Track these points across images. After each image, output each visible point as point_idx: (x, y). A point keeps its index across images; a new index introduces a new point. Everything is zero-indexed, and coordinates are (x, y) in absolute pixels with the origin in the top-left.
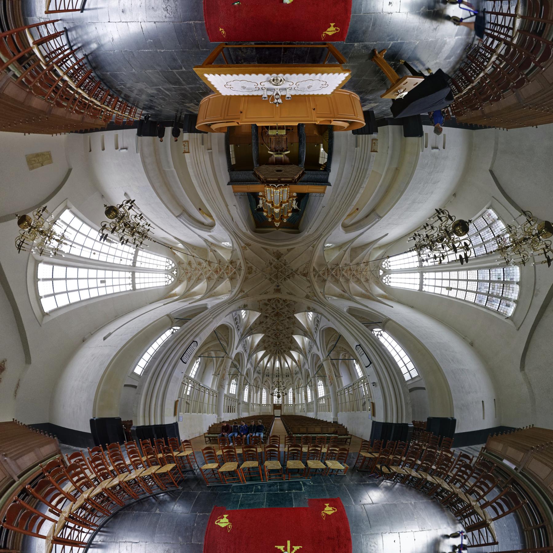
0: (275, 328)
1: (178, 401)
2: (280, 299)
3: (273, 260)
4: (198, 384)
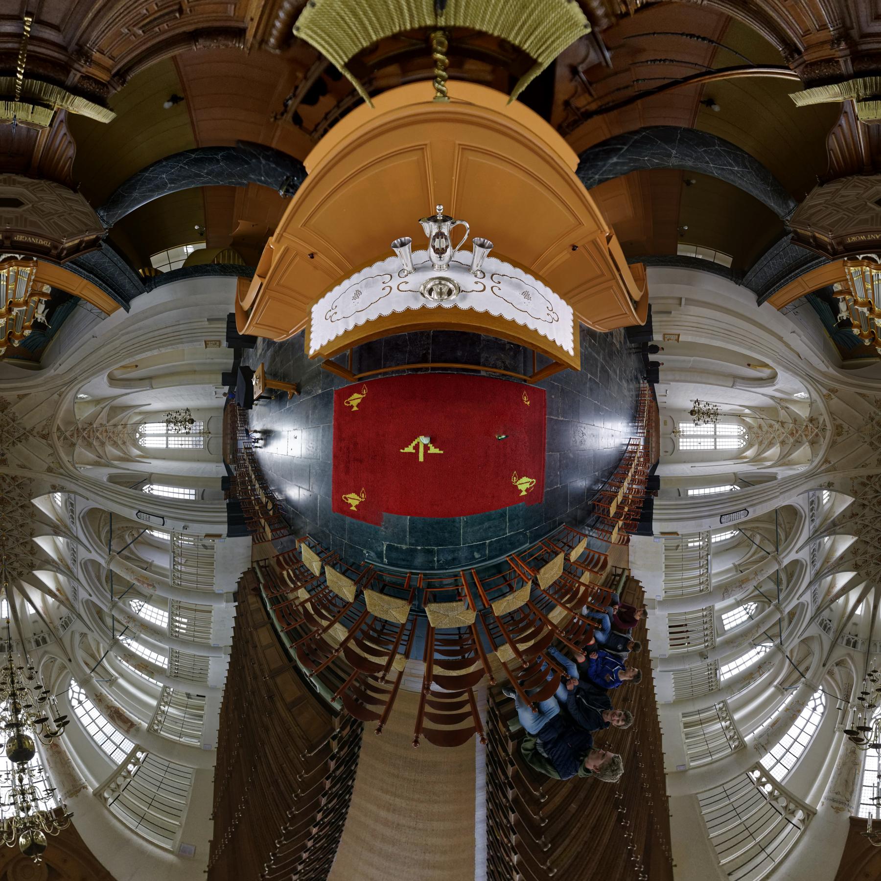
1: (678, 535)
4: (708, 553)
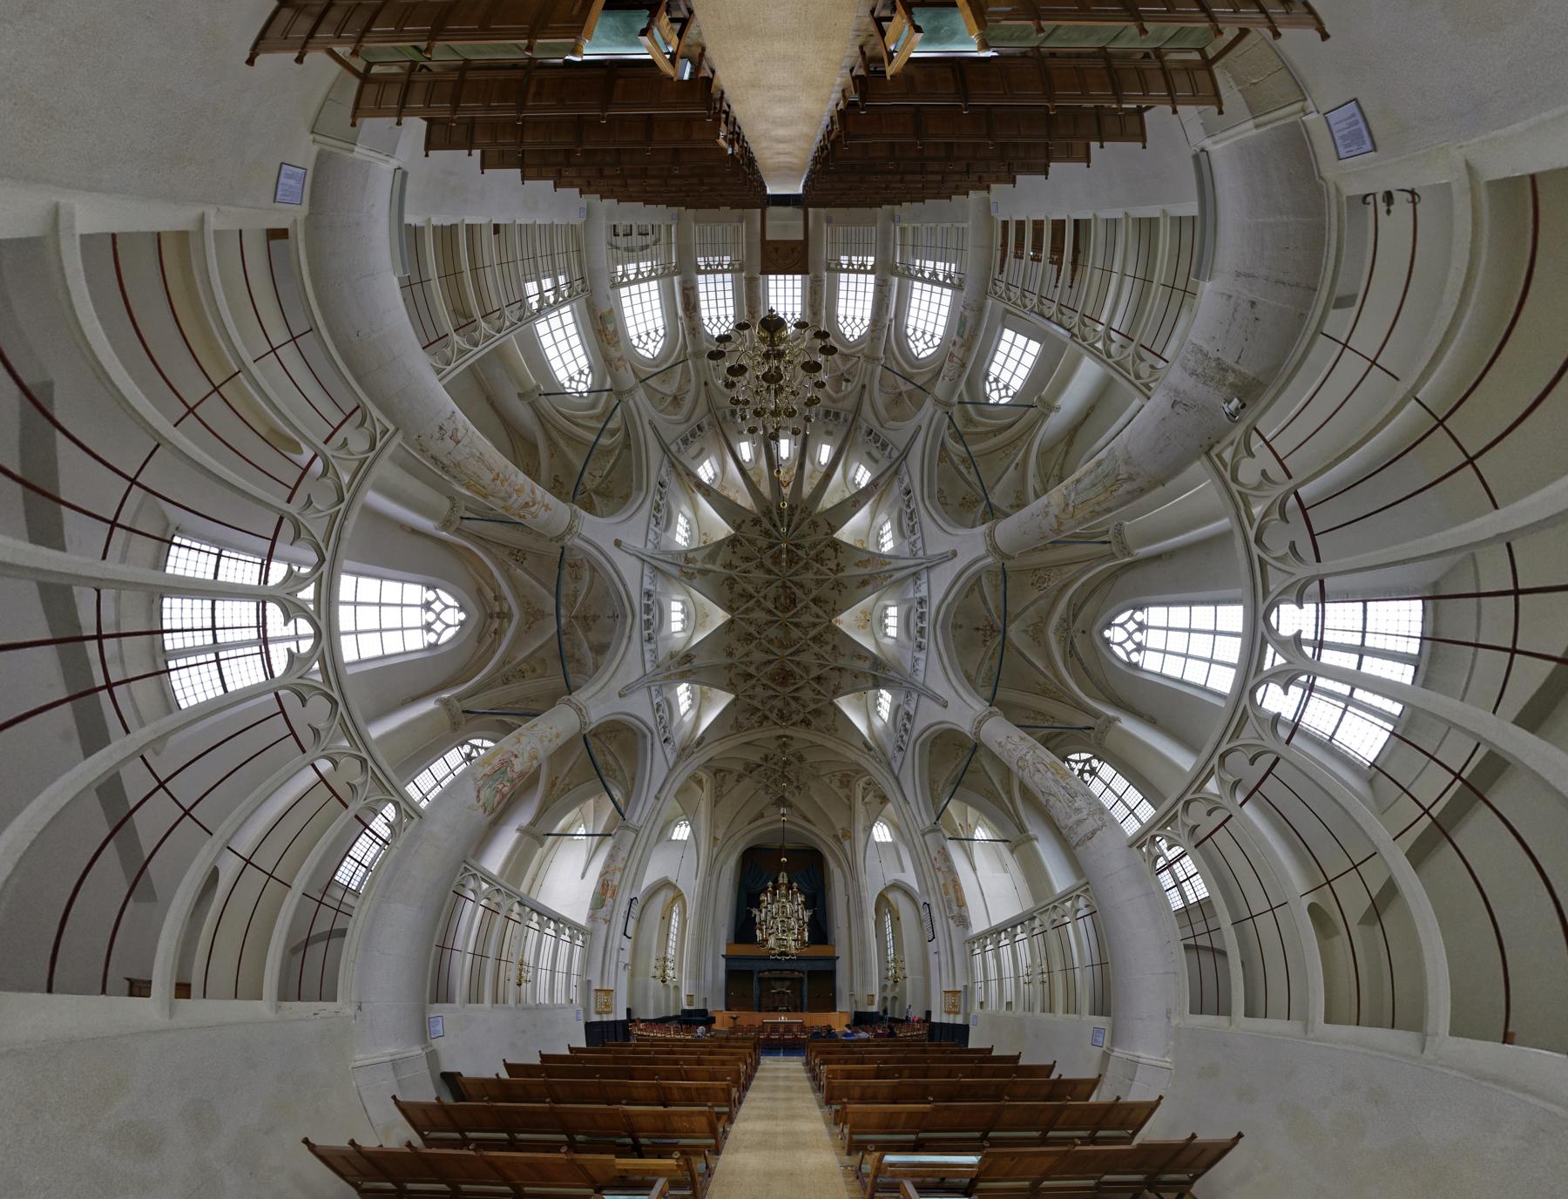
0: (796, 633)
2: (776, 724)
3: (794, 794)
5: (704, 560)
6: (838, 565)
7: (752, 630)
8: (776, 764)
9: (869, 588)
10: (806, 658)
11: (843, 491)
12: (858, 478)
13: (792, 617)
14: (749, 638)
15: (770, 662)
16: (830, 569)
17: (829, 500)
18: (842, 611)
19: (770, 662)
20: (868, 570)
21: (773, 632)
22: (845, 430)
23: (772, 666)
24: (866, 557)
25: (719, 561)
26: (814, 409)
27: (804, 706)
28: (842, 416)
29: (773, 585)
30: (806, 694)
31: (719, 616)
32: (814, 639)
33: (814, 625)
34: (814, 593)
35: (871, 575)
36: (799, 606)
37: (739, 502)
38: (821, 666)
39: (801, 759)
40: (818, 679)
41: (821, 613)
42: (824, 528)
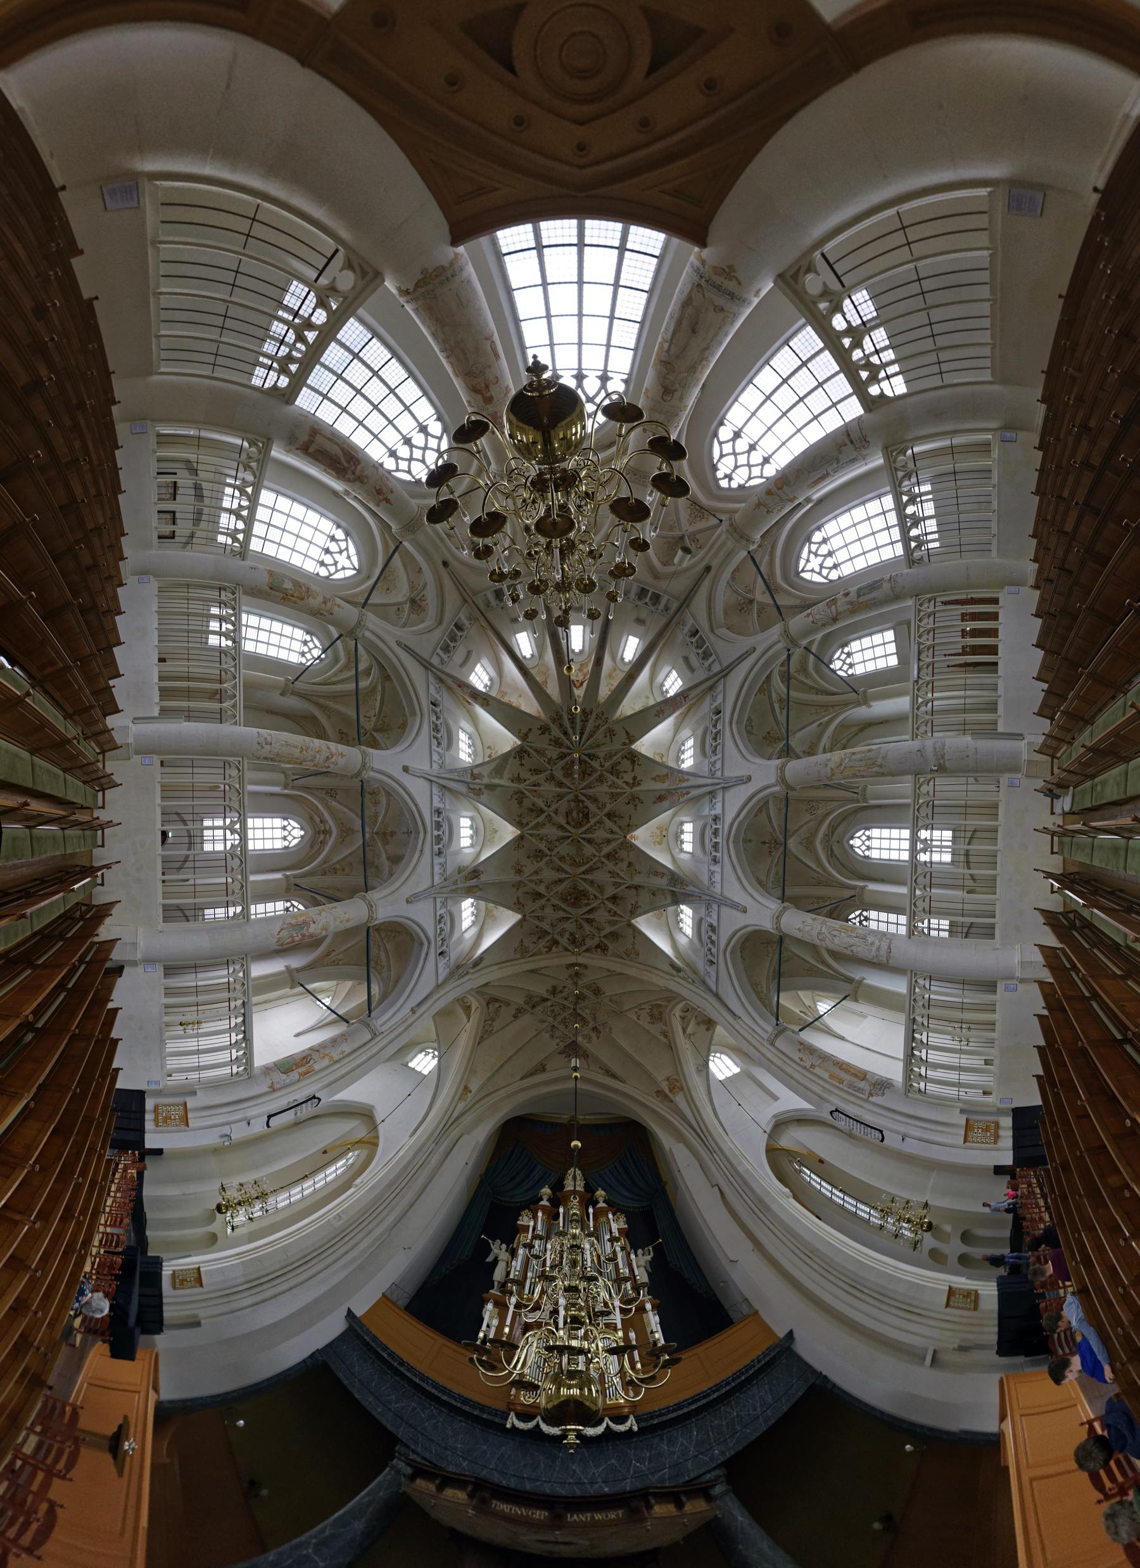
0: (589, 850)
2: (567, 950)
5: (490, 775)
6: (635, 778)
7: (542, 846)
8: (566, 999)
9: (666, 803)
10: (601, 876)
11: (647, 697)
12: (667, 684)
13: (585, 833)
14: (539, 855)
15: (561, 881)
16: (626, 783)
17: (629, 706)
18: (637, 827)
19: (561, 881)
20: (665, 786)
21: (564, 849)
22: (663, 621)
23: (564, 885)
24: (665, 771)
25: (506, 775)
26: (623, 582)
27: (599, 929)
28: (663, 601)
29: (566, 798)
30: (601, 916)
31: (508, 832)
32: (608, 856)
33: (609, 841)
34: (609, 807)
35: (668, 790)
36: (593, 821)
37: (523, 708)
38: (617, 885)
39: (597, 992)
40: (614, 899)
41: (616, 829)
42: (621, 737)
